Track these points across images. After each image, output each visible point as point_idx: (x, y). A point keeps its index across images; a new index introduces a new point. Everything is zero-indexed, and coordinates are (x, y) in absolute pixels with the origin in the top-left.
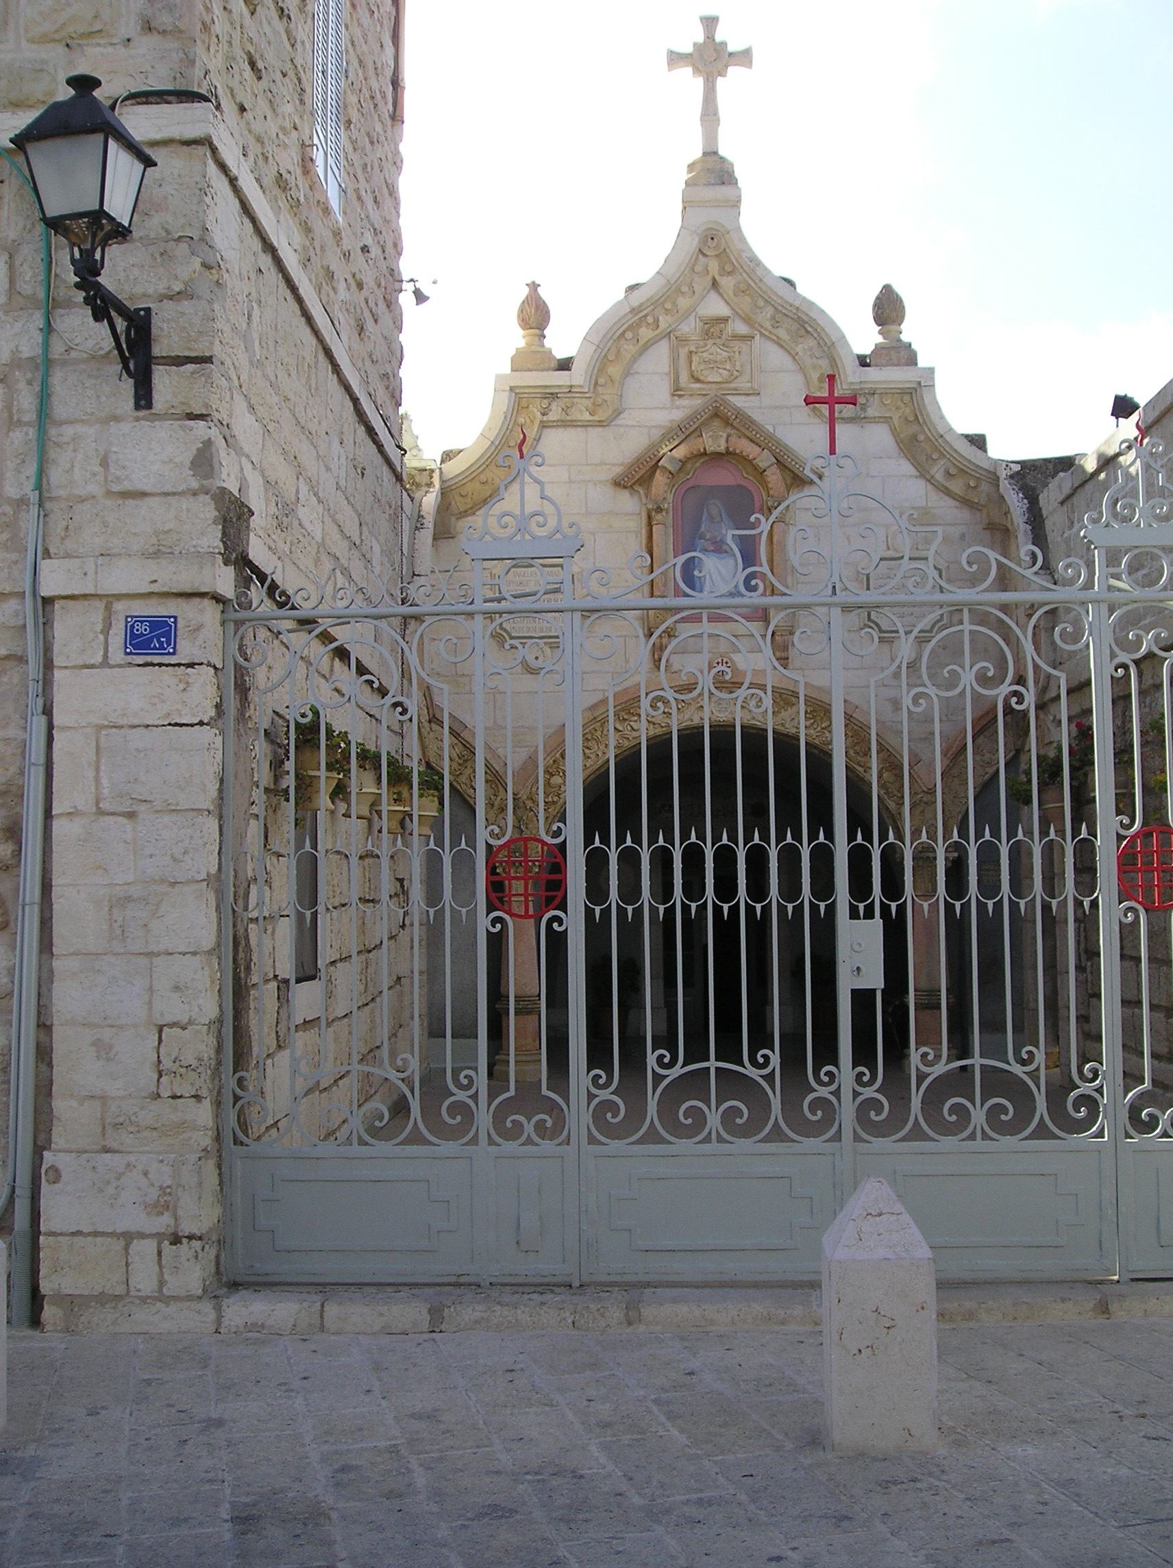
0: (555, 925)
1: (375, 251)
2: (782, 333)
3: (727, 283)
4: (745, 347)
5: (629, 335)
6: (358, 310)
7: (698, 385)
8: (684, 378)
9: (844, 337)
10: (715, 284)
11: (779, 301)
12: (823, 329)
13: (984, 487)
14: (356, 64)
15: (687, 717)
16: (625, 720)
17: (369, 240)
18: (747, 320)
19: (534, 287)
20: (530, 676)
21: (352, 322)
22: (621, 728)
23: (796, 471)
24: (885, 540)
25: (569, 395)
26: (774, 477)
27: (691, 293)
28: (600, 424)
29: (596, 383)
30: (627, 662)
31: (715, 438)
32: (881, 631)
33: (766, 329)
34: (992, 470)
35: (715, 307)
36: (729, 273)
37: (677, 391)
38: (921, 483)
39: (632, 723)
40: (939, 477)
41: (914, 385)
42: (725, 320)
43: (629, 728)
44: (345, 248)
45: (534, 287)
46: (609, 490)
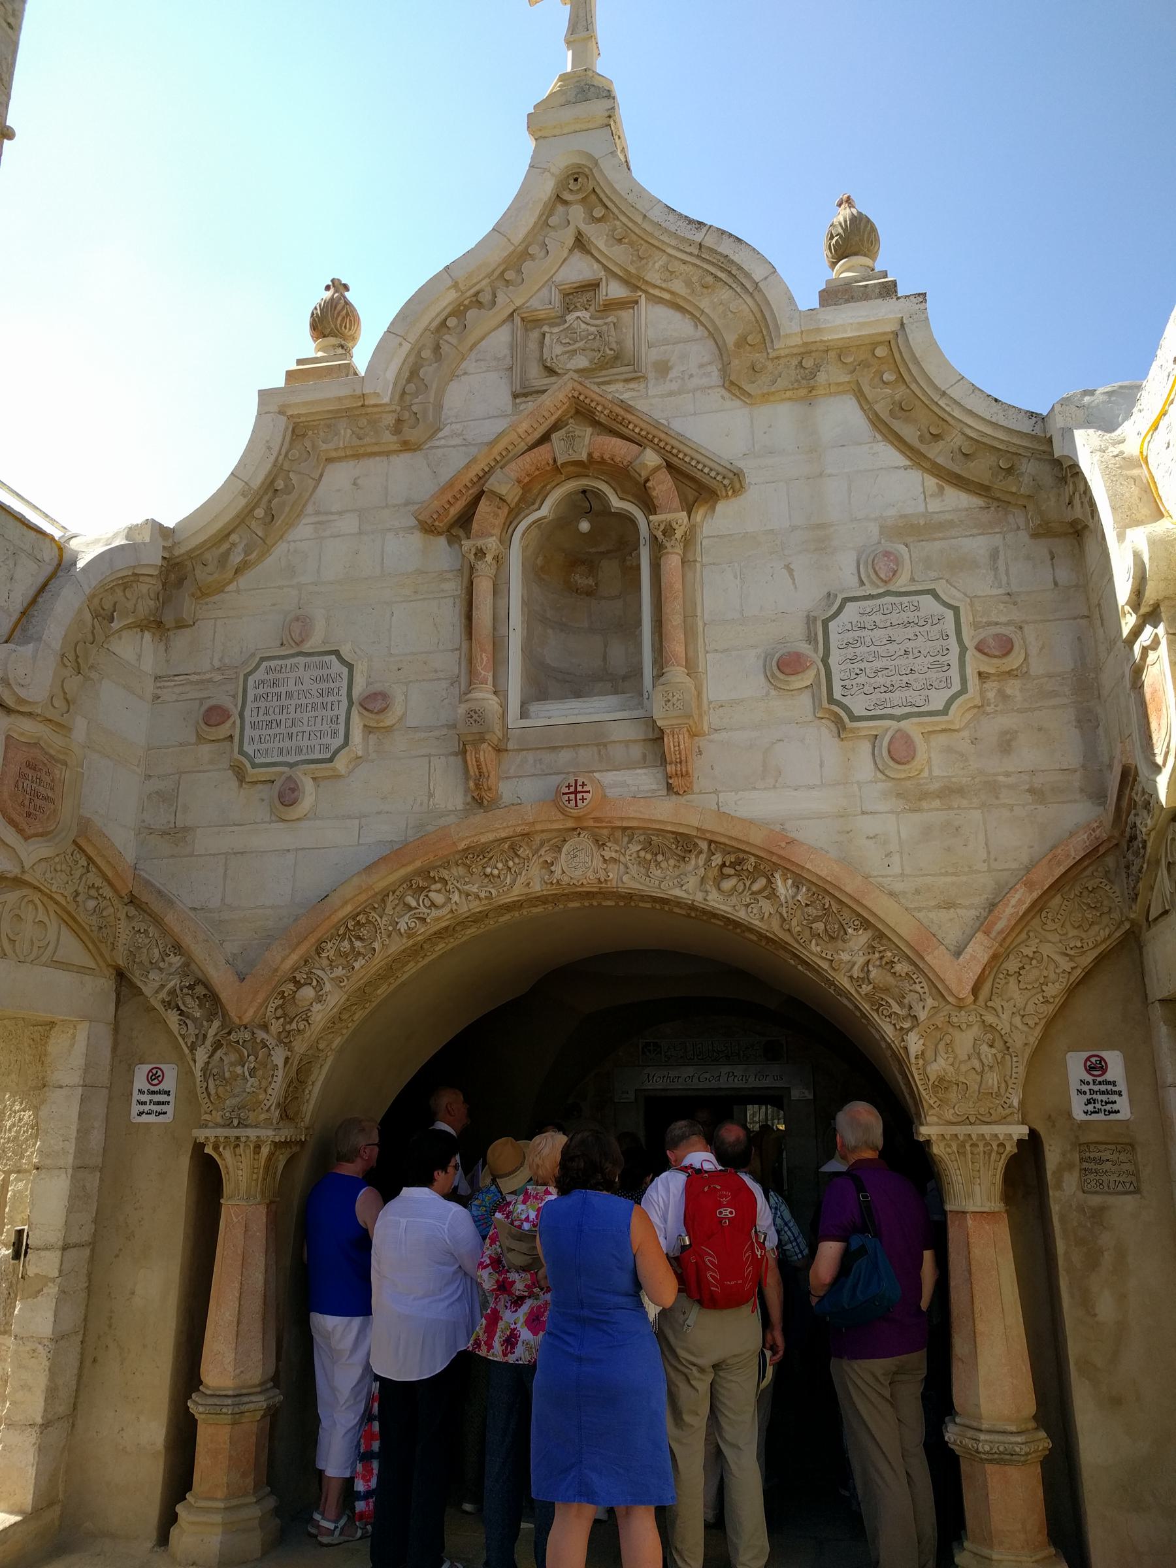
2: (678, 286)
3: (598, 237)
4: (626, 315)
5: (452, 322)
8: (534, 372)
9: (775, 271)
10: (581, 243)
11: (673, 243)
12: (740, 268)
13: (1029, 468)
16: (423, 889)
18: (628, 281)
20: (282, 825)
22: (413, 904)
23: (698, 475)
24: (855, 572)
25: (363, 411)
26: (663, 487)
27: (543, 253)
28: (408, 447)
29: (404, 393)
30: (431, 795)
32: (853, 718)
33: (655, 286)
34: (1038, 431)
35: (579, 269)
36: (599, 220)
39: (431, 894)
41: (895, 327)
42: (594, 286)
43: (427, 903)
46: (417, 539)
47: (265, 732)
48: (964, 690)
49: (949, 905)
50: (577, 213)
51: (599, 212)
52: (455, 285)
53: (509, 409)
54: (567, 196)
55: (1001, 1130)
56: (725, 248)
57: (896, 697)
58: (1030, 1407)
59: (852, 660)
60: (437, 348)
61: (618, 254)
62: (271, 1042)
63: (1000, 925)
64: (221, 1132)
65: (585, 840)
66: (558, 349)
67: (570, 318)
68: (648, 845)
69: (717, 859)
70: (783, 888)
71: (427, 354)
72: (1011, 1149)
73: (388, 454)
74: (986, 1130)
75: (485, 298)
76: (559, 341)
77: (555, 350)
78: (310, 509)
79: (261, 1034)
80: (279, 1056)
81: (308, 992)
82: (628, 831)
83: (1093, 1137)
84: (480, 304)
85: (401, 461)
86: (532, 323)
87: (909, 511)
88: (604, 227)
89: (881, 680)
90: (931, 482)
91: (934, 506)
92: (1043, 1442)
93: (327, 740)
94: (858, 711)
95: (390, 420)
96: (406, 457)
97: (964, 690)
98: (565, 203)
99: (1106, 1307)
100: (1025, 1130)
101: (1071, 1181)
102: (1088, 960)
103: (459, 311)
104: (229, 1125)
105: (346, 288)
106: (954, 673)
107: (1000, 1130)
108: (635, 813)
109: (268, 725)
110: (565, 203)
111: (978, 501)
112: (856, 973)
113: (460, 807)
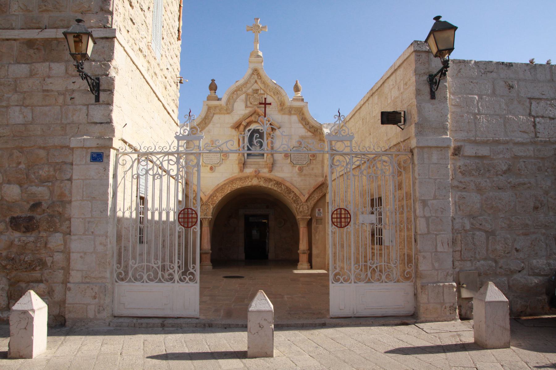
0: (195, 230)
1: (170, 69)
3: (259, 81)
5: (235, 93)
6: (165, 83)
7: (252, 105)
8: (248, 103)
10: (256, 82)
14: (166, 25)
15: (247, 183)
17: (169, 67)
18: (263, 90)
19: (213, 80)
21: (163, 86)
28: (228, 113)
29: (227, 104)
31: (255, 117)
32: (294, 164)
35: (256, 87)
37: (246, 107)
38: (304, 129)
40: (308, 128)
42: (258, 90)
44: (161, 68)
45: (213, 80)
46: (230, 129)
47: (207, 159)
48: (308, 162)
49: (304, 190)
50: (256, 77)
51: (259, 78)
52: (236, 87)
53: (244, 109)
54: (254, 73)
55: (307, 217)
56: (280, 89)
57: (299, 162)
58: (308, 248)
59: (294, 156)
60: (233, 97)
61: (262, 86)
62: (210, 204)
63: (310, 192)
64: (204, 217)
65: (256, 179)
66: (252, 100)
67: (255, 95)
68: (265, 180)
69: (275, 182)
70: (283, 186)
71: (231, 98)
72: (309, 220)
73: (225, 114)
74: (306, 217)
75: (241, 89)
76: (253, 99)
77: (252, 100)
78: (212, 122)
79: (209, 204)
80: (211, 207)
81: (215, 198)
82: (263, 177)
83: (318, 218)
84: (240, 91)
85: (227, 116)
86: (247, 95)
87: (303, 134)
88: (260, 80)
89: (298, 159)
90: (306, 131)
91: (306, 134)
92: (309, 252)
93: (217, 161)
94: (294, 163)
95: (225, 108)
96: (228, 115)
97: (308, 162)
98: (254, 74)
99: (317, 237)
100: (310, 217)
101: (315, 223)
102: (320, 197)
103: (236, 91)
104: (204, 216)
105: (215, 80)
106: (307, 159)
107: (307, 217)
108: (264, 175)
109: (207, 158)
110: (254, 74)
111: (312, 134)
112: (292, 198)
113: (237, 172)
